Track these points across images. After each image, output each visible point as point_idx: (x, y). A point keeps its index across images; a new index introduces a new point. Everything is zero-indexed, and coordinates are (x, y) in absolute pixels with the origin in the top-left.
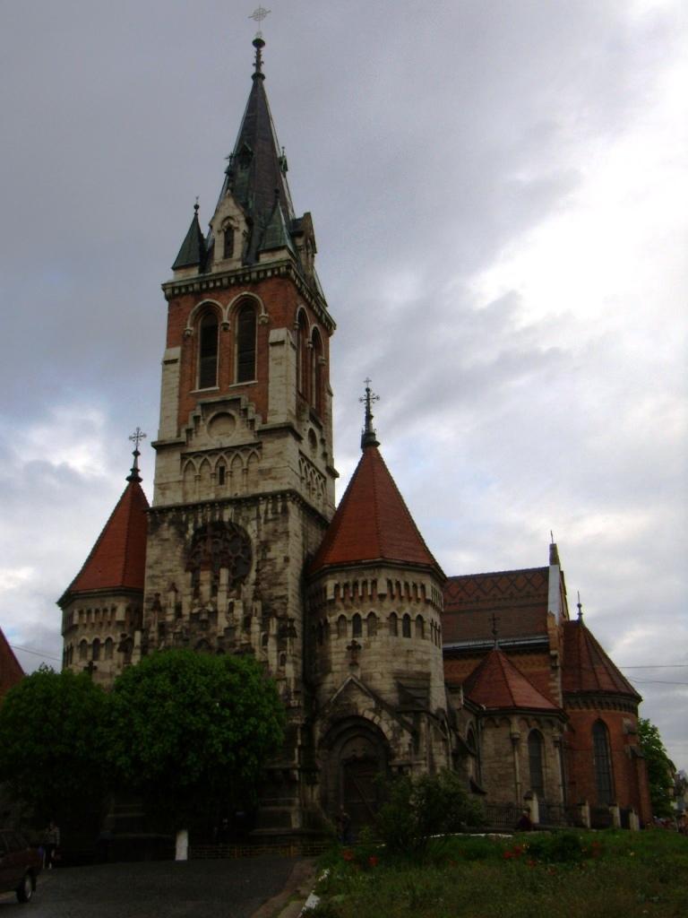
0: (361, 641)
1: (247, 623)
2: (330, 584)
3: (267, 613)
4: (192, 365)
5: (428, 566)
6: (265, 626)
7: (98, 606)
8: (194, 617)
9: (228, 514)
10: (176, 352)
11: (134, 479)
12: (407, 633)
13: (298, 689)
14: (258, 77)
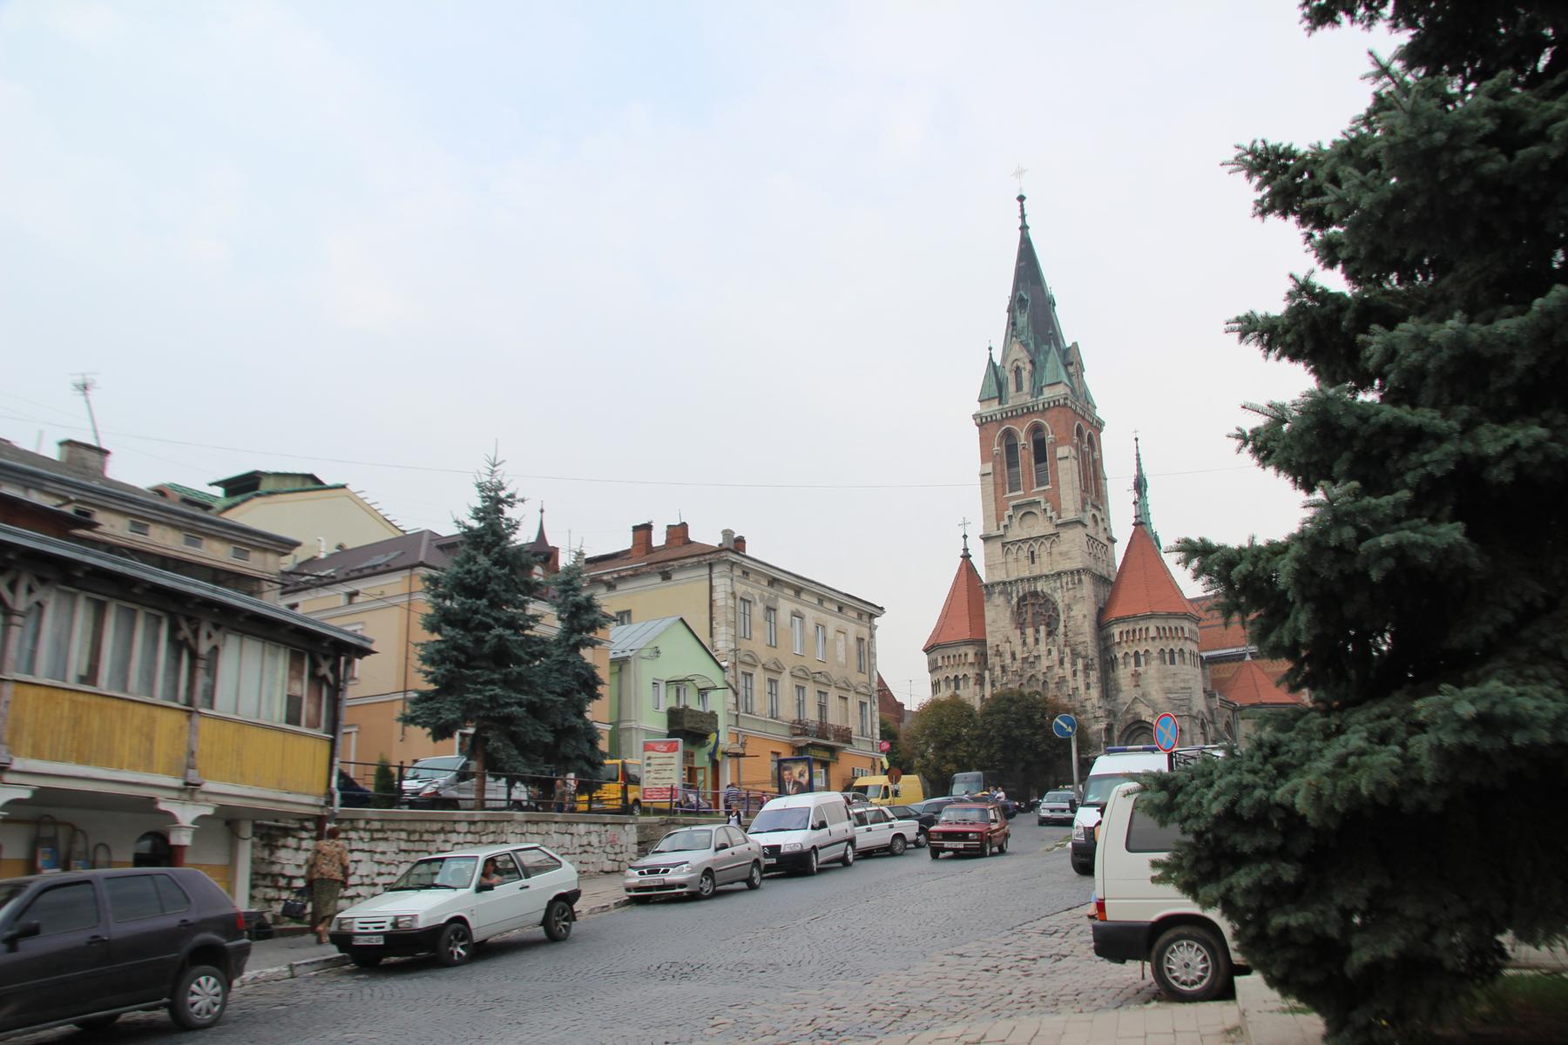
0: (1140, 670)
1: (1061, 662)
2: (1116, 630)
3: (1075, 654)
4: (1002, 475)
5: (1185, 614)
6: (1074, 664)
7: (955, 653)
8: (1025, 660)
9: (1040, 586)
10: (989, 468)
11: (966, 557)
12: (1172, 662)
13: (1101, 705)
14: (1024, 228)
